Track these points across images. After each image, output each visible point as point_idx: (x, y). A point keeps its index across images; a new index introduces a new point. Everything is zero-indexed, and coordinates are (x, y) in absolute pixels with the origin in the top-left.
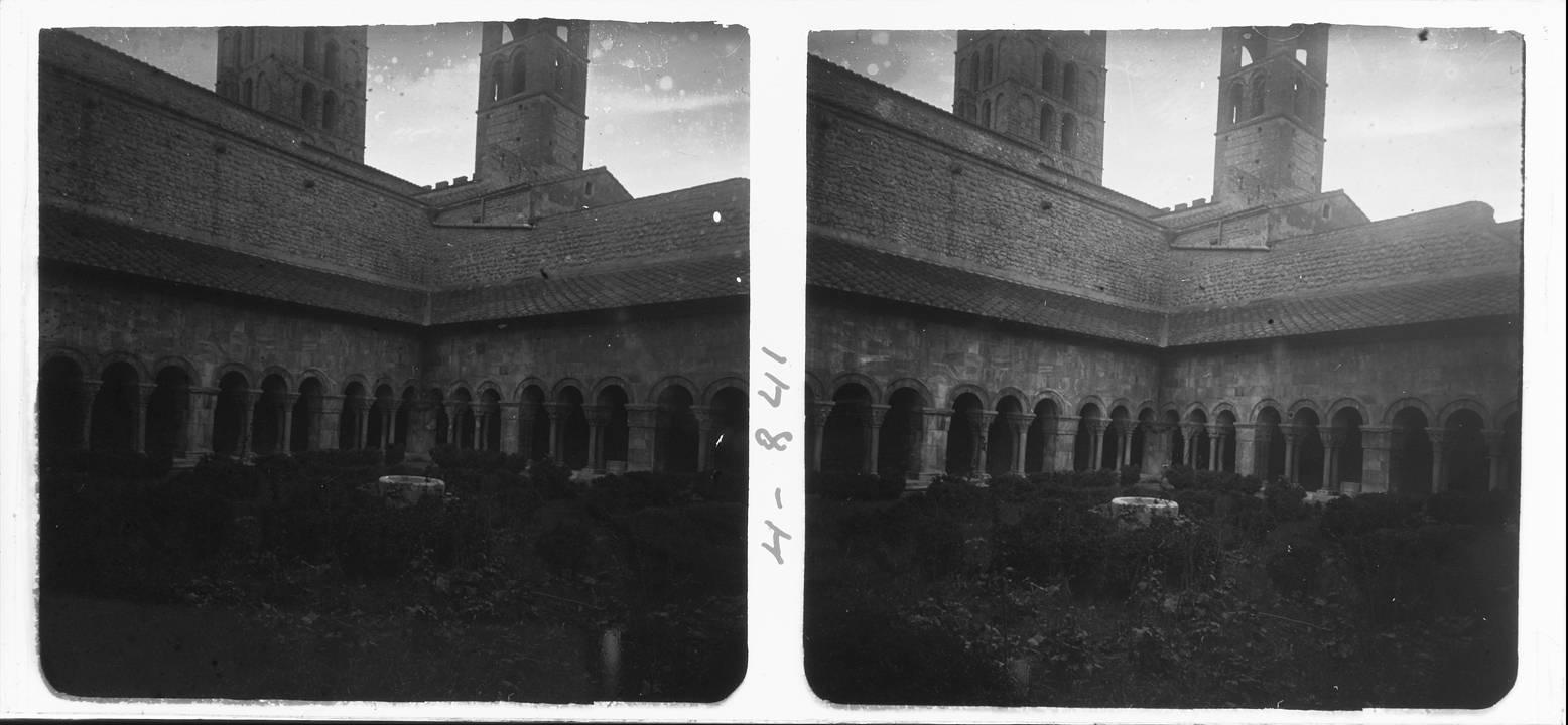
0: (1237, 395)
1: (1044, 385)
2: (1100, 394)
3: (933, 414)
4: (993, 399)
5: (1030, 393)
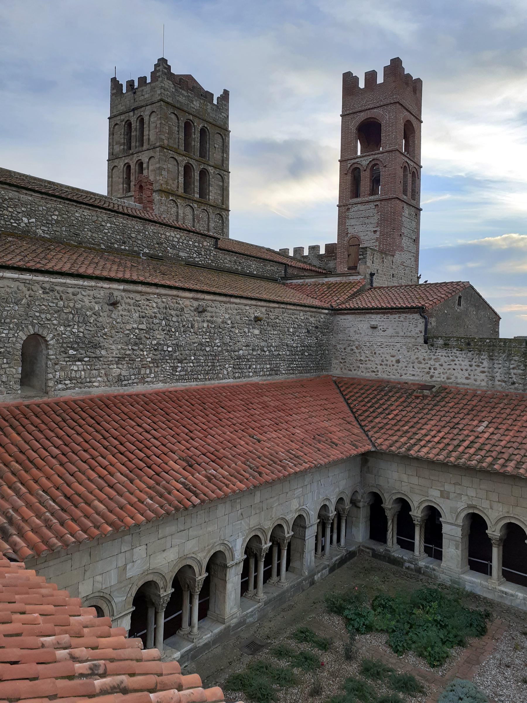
0: (442, 496)
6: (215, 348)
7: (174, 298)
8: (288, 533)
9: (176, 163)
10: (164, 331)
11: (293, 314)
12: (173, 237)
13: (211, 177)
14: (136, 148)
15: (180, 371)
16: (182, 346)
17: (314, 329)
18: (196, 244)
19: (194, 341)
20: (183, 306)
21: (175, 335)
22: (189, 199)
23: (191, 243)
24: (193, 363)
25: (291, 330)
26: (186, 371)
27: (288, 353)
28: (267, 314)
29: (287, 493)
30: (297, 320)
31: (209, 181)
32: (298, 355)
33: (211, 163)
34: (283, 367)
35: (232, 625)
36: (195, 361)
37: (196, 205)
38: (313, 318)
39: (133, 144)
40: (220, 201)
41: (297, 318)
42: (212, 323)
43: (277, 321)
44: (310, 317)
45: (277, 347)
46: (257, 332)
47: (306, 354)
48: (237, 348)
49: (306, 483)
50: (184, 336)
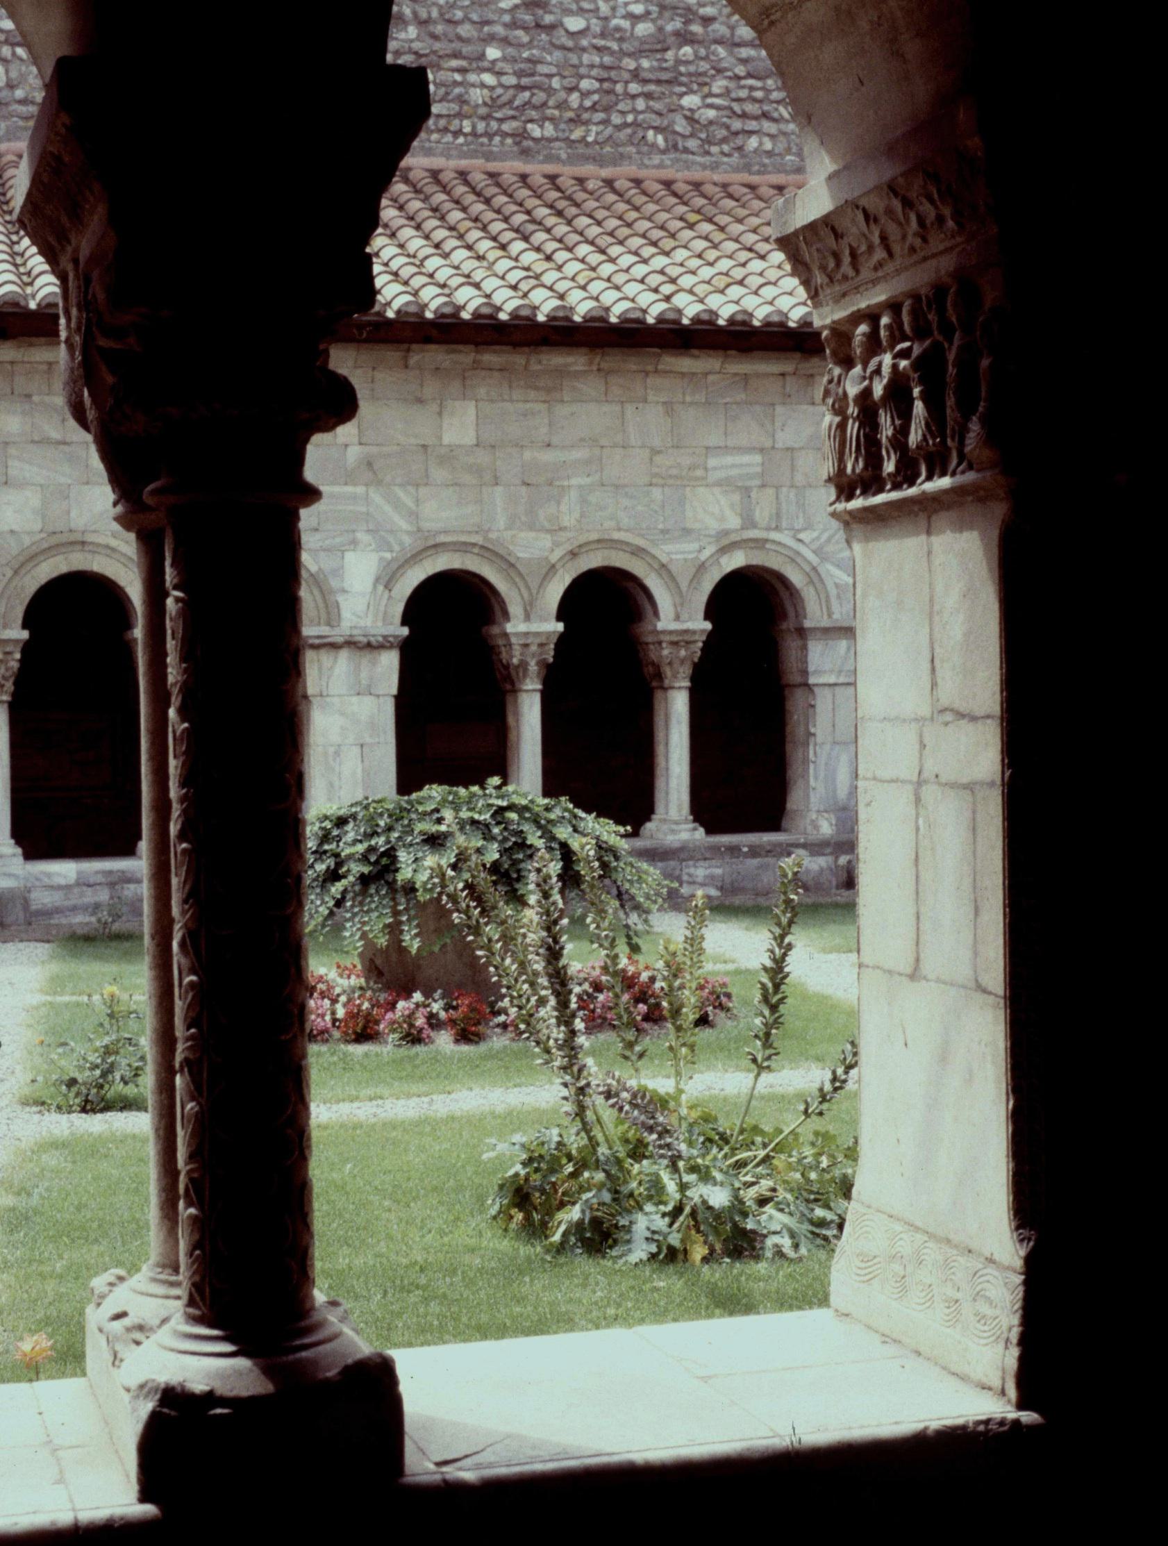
1: (734, 522)
3: (334, 646)
5: (677, 552)
24: (499, 74)
26: (462, 100)
29: (655, 452)
36: (508, 68)
49: (785, 438)
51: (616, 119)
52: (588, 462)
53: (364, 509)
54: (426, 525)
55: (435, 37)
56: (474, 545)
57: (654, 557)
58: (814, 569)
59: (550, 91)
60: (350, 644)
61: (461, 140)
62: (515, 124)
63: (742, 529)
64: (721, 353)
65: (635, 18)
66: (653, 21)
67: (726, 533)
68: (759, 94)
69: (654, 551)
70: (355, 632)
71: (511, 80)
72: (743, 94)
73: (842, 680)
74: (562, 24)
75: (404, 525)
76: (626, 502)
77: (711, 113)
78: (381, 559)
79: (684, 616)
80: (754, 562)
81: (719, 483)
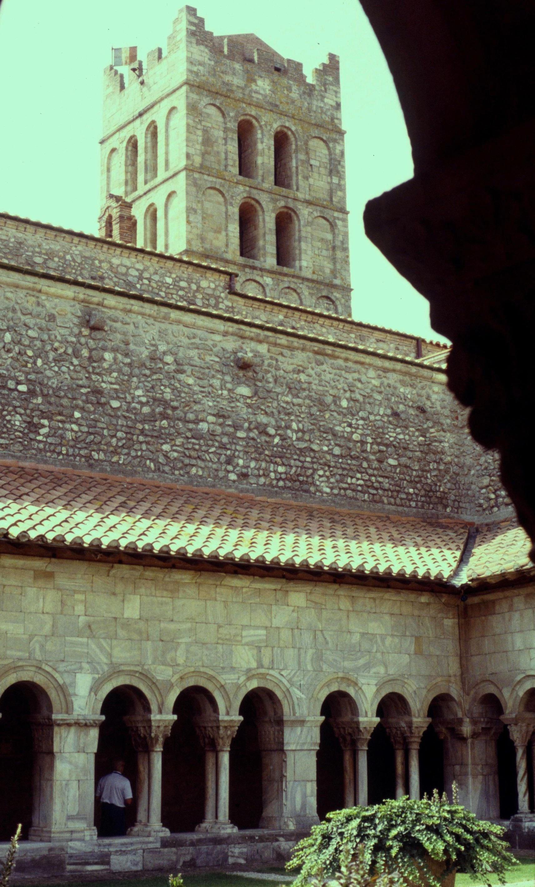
1: (254, 665)
2: (353, 676)
3: (69, 725)
4: (169, 691)
5: (228, 679)
6: (133, 405)
7: (31, 292)
8: (228, 713)
9: (221, 199)
10: (9, 351)
11: (348, 370)
12: (128, 268)
13: (302, 222)
14: (146, 183)
15: (47, 436)
16: (51, 387)
17: (412, 411)
18: (183, 284)
19: (80, 382)
20: (54, 312)
21: (35, 363)
22: (254, 268)
23: (169, 280)
24: (80, 425)
25: (344, 403)
26: (62, 437)
27: (337, 451)
28: (271, 358)
29: (219, 626)
30: (359, 385)
31: (300, 231)
32: (366, 459)
33: (300, 195)
34: (324, 479)
35: (70, 851)
36: (84, 423)
37: (268, 280)
38: (408, 390)
39: (141, 178)
40: (328, 271)
41: (360, 381)
42: (126, 355)
43: (303, 377)
44: (398, 385)
45: (303, 432)
46: (244, 390)
47: (392, 462)
48: (191, 416)
50: (56, 369)
51: (133, 453)
52: (190, 630)
53: (86, 651)
54: (114, 660)
55: (50, 404)
56: (136, 672)
57: (218, 681)
58: (288, 690)
59: (103, 436)
60: (77, 724)
61: (61, 457)
62: (86, 451)
63: (258, 668)
64: (251, 577)
65: (142, 404)
66: (150, 406)
67: (249, 670)
68: (197, 447)
69: (219, 678)
70: (80, 718)
71: (85, 429)
72: (190, 446)
73: (298, 748)
74: (109, 403)
75: (105, 660)
76: (206, 652)
77: (175, 454)
78: (93, 678)
79: (231, 713)
80: (262, 685)
81: (247, 644)
